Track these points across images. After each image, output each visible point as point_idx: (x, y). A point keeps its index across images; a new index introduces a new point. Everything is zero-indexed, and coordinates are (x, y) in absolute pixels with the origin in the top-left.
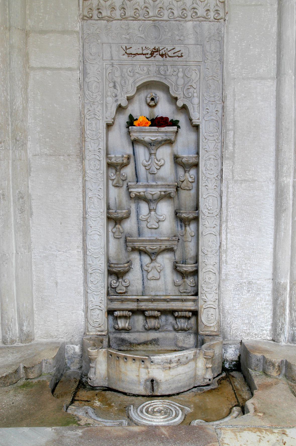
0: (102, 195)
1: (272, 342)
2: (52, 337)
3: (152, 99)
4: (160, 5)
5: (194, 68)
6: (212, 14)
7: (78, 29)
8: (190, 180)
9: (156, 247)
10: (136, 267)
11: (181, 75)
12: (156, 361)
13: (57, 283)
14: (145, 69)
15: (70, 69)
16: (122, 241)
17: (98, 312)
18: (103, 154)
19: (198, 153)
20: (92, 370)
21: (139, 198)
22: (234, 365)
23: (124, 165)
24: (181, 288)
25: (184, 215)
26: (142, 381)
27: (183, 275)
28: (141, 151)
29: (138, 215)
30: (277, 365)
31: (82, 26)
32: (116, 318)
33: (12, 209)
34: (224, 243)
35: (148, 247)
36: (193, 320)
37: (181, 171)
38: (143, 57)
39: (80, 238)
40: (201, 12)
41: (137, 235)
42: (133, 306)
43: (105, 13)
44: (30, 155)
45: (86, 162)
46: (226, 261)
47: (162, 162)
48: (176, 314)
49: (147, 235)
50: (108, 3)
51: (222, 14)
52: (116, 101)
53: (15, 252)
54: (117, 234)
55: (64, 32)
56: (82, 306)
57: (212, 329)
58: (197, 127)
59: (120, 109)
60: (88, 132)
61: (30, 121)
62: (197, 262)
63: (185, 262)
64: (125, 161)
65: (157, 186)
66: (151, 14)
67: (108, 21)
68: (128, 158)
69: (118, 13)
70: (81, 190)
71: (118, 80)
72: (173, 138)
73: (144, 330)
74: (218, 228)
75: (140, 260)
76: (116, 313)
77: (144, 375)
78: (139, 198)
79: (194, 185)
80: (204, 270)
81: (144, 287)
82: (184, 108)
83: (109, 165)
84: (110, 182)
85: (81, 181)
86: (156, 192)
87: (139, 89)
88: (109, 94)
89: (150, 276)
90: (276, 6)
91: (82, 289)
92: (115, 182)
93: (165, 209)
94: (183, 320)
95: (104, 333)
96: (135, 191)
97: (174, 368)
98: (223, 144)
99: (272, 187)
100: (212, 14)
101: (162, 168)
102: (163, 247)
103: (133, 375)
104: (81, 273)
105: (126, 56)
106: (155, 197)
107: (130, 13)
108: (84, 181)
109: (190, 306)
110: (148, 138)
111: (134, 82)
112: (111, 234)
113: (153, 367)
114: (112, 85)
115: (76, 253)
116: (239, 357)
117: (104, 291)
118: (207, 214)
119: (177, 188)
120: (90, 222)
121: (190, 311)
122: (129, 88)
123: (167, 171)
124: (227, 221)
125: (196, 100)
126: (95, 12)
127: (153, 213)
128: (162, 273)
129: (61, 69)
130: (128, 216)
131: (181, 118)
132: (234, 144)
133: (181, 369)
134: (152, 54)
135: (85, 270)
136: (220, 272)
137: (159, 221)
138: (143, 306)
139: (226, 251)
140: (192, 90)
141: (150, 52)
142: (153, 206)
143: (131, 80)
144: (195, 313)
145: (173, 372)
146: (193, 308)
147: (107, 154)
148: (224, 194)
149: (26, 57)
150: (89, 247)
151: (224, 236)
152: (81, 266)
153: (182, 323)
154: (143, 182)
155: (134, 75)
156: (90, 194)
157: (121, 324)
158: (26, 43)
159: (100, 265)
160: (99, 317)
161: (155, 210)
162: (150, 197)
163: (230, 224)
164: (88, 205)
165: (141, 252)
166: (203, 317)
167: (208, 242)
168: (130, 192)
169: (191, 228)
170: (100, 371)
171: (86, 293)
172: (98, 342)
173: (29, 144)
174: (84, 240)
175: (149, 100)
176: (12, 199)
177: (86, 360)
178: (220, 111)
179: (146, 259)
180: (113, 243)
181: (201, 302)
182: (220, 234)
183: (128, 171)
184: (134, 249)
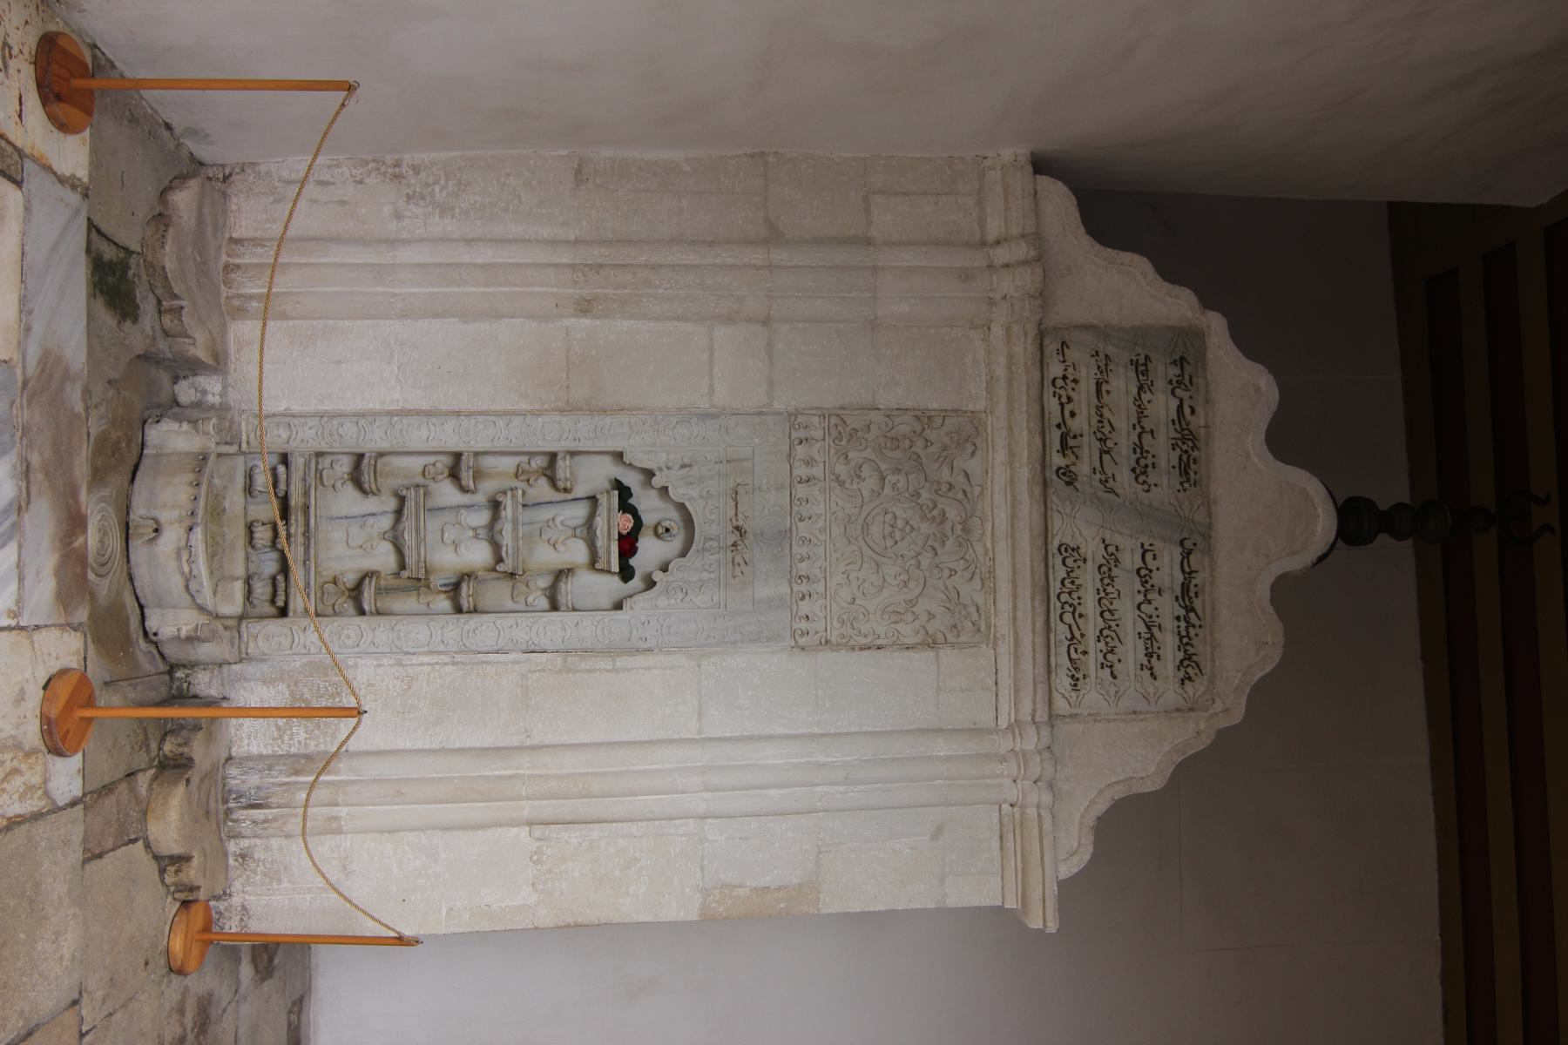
0: (500, 445)
1: (224, 755)
2: (239, 351)
3: (667, 530)
4: (814, 540)
5: (716, 598)
6: (804, 625)
7: (777, 406)
8: (530, 599)
9: (409, 538)
10: (371, 504)
11: (705, 576)
12: (192, 535)
13: (339, 362)
14: (713, 517)
15: (712, 391)
16: (420, 480)
17: (284, 434)
18: (573, 446)
19: (574, 610)
20: (174, 426)
21: (495, 506)
22: (180, 688)
23: (553, 481)
24: (330, 587)
25: (464, 586)
26: (156, 513)
27: (356, 592)
28: (579, 512)
29: (467, 507)
30: (186, 750)
31: (780, 414)
32: (274, 470)
33: (473, 289)
34: (414, 659)
35: (408, 524)
36: (268, 609)
37: (544, 582)
38: (731, 513)
39: (423, 405)
40: (805, 607)
41: (429, 505)
42: (295, 500)
43: (800, 450)
44: (567, 322)
45: (556, 417)
46: (380, 665)
47: (561, 548)
48: (280, 578)
49: (433, 524)
50: (817, 457)
51: (802, 641)
52: (660, 469)
53: (397, 291)
54: (432, 469)
55: (771, 383)
56: (296, 408)
57: (251, 645)
58: (618, 606)
59: (649, 474)
60: (608, 420)
61: (625, 325)
62: (379, 613)
63: (379, 591)
64: (561, 484)
65: (515, 539)
66: (800, 525)
67: (789, 455)
68: (566, 490)
69: (801, 471)
70: (509, 407)
71: (694, 471)
72: (598, 566)
73: (250, 519)
74: (442, 648)
75: (385, 512)
76: (281, 469)
77: (165, 516)
78: (495, 506)
79: (521, 607)
80: (364, 626)
81: (331, 518)
82: (650, 584)
83: (553, 457)
84: (525, 459)
85: (524, 406)
86: (507, 539)
87: (682, 507)
88: (672, 457)
89: (354, 530)
90: (816, 731)
91: (328, 406)
92: (525, 466)
93: (477, 555)
94: (269, 589)
95: (244, 446)
96: (508, 502)
97: (180, 568)
98: (588, 652)
99: (515, 741)
100: (804, 625)
101: (551, 549)
102: (407, 552)
103: (165, 498)
104: (359, 406)
105: (732, 484)
106: (498, 537)
107: (801, 491)
108: (523, 414)
109: (297, 603)
110: (600, 522)
111: (691, 499)
112: (431, 459)
113: (182, 530)
114: (687, 461)
115: (394, 397)
116: (195, 696)
117: (324, 447)
118: (467, 627)
119: (512, 574)
120: (451, 424)
121: (286, 602)
122: (681, 491)
123: (546, 556)
124: (454, 664)
125: (663, 602)
126: (802, 434)
127: (471, 533)
128: (360, 551)
129: (711, 376)
130: (464, 490)
131: (636, 583)
132: (589, 671)
133: (177, 582)
134: (737, 528)
135: (363, 415)
136: (360, 655)
137: (456, 545)
138: (297, 518)
139: (399, 663)
140: (680, 595)
141: (740, 523)
142: (483, 533)
143: (694, 492)
144: (283, 612)
145: (172, 564)
146: (291, 606)
147: (573, 454)
148: (502, 657)
149: (729, 319)
150: (405, 421)
151: (426, 659)
152: (371, 406)
153: (262, 590)
154: (524, 516)
155: (701, 497)
156: (501, 423)
157: (262, 480)
158: (749, 320)
159: (375, 439)
160: (278, 438)
161: (476, 537)
162: (498, 527)
163: (449, 669)
164: (481, 419)
165: (399, 512)
166: (275, 627)
167: (418, 632)
168: (505, 493)
169: (444, 603)
170: (170, 437)
171: (321, 415)
172: (230, 436)
173: (586, 322)
174: (419, 413)
175: (666, 524)
176: (489, 290)
177: (193, 413)
178: (645, 646)
179: (386, 522)
180: (416, 463)
181: (305, 622)
182: (431, 653)
183: (542, 489)
184: (402, 500)
